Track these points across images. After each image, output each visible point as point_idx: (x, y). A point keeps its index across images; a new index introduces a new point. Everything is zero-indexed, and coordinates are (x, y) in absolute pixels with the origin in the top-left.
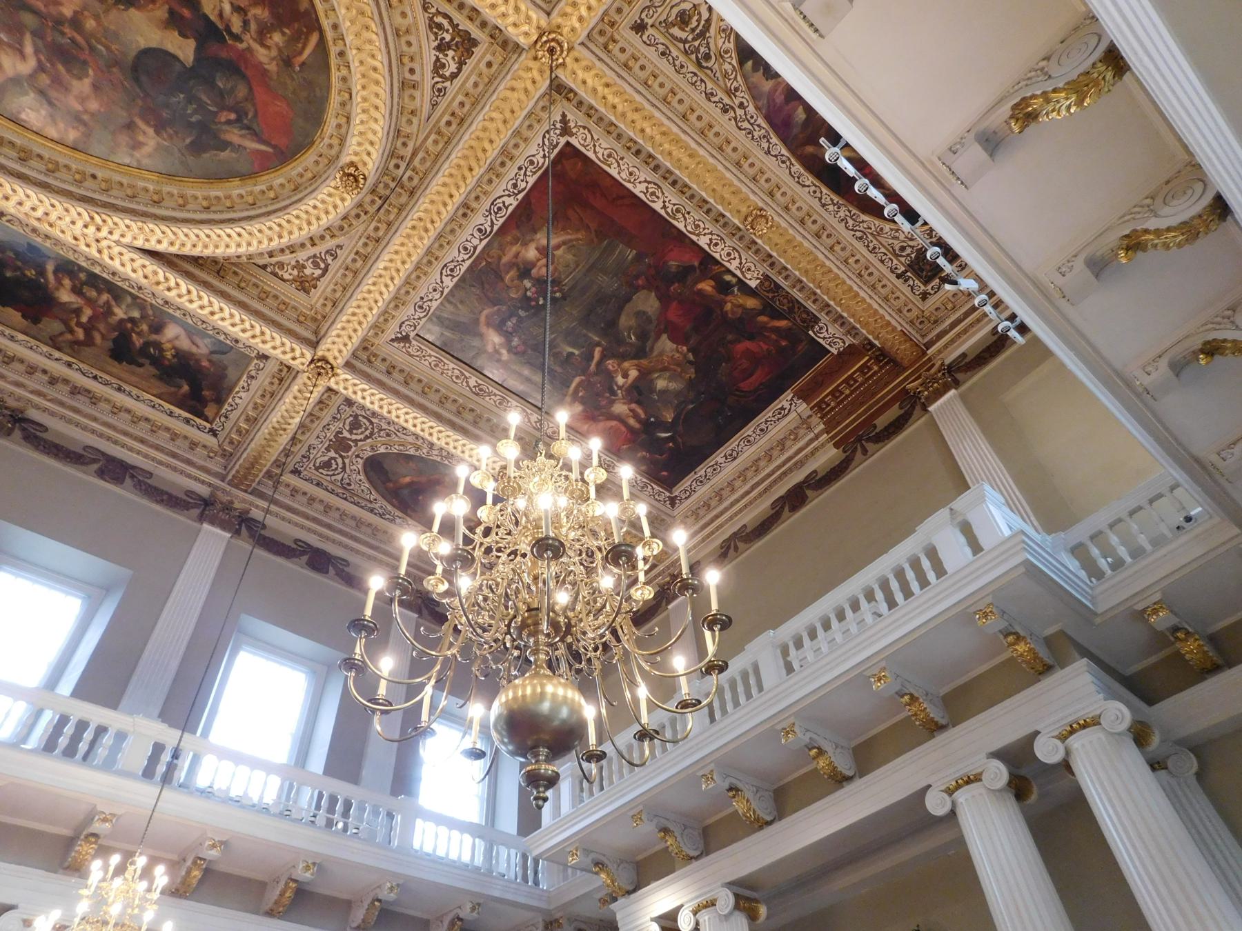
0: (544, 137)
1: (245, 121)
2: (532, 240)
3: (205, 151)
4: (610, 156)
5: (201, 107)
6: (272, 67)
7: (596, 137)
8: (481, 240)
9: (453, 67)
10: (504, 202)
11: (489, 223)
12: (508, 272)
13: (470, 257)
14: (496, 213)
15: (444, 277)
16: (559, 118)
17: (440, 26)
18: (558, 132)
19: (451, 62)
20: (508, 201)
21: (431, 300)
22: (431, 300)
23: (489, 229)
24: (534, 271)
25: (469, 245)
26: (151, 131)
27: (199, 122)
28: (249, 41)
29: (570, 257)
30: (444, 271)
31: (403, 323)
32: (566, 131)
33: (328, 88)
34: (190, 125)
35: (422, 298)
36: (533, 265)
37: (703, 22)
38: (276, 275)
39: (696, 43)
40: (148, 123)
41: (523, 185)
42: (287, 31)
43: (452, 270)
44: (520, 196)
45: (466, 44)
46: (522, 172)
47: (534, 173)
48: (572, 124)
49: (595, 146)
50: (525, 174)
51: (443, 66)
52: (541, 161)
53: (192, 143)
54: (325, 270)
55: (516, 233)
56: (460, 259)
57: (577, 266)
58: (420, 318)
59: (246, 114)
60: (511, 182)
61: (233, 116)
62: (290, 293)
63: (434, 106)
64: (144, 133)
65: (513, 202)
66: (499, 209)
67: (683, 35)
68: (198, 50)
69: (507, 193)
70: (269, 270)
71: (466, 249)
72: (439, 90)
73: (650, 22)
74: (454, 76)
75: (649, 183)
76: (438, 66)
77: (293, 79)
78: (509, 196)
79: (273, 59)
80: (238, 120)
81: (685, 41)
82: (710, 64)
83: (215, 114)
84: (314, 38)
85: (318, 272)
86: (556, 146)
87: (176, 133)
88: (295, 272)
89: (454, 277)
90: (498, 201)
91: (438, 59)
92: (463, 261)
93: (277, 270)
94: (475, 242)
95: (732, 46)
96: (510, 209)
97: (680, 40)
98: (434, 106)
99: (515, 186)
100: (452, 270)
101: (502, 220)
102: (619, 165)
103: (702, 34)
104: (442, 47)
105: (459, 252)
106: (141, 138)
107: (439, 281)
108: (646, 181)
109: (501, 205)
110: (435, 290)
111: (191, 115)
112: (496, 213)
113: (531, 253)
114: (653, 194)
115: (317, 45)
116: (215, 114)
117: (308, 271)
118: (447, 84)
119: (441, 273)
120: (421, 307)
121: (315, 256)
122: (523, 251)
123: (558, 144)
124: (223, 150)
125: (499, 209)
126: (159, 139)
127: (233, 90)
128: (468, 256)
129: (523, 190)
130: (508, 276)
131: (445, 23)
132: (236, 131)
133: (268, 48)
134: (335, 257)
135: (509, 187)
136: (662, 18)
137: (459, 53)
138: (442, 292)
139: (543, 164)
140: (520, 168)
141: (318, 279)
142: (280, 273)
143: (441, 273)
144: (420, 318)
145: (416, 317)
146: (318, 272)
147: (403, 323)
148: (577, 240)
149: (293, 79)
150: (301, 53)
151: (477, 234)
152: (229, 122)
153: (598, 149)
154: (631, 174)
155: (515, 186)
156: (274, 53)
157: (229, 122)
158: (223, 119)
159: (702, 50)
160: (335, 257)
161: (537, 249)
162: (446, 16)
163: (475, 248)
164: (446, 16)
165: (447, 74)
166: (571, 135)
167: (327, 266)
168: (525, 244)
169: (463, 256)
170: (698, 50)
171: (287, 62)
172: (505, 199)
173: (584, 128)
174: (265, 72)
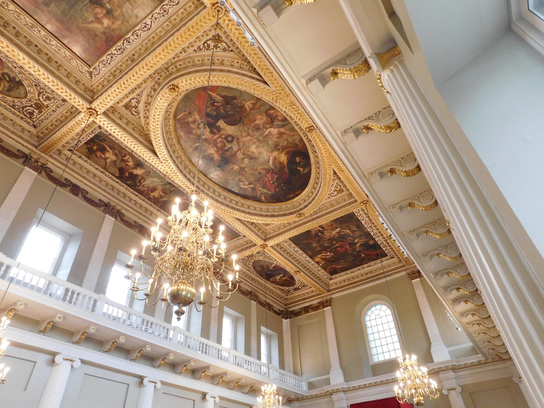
0: (99, 73)
1: (212, 101)
2: (106, 28)
3: (231, 97)
4: (70, 60)
5: (224, 110)
6: (195, 113)
7: (77, 68)
8: (129, 38)
9: (133, 101)
10: (117, 52)
11: (125, 45)
12: (119, 15)
13: (136, 31)
14: (121, 48)
15: (150, 24)
16: (93, 78)
17: (136, 112)
18: (93, 73)
19: (133, 102)
20: (115, 52)
21: (159, 14)
22: (159, 14)
23: (125, 42)
24: (105, 12)
25: (136, 37)
26: (246, 106)
27: (228, 105)
28: (200, 121)
29: (86, 15)
30: (149, 27)
31: (176, 4)
32: (91, 73)
33: (178, 104)
34: (231, 105)
35: (163, 16)
36: (105, 15)
37: (41, 96)
38: (228, 46)
39: (41, 91)
40: (246, 108)
41: (108, 57)
42: (186, 120)
43: (145, 27)
44: (109, 52)
45: (127, 106)
46: (108, 62)
47: (103, 60)
48: (88, 75)
49: (77, 65)
50: (107, 61)
51: (136, 102)
52: (100, 64)
53: (235, 100)
54: (206, 42)
55: (114, 34)
56: (140, 31)
57: (81, 9)
58: (167, 5)
59: (211, 103)
60: (114, 59)
61: (216, 104)
62: (224, 38)
63: (142, 92)
64: (249, 107)
65: (113, 50)
66: (119, 50)
67: (47, 94)
68: (217, 122)
69: (116, 55)
70: (230, 49)
71: (137, 35)
72: (139, 96)
73: (61, 101)
74: (133, 99)
75: (50, 44)
76: (138, 102)
77: (190, 109)
78: (115, 54)
79: (195, 115)
80: (214, 102)
81: (46, 92)
82: (33, 83)
83: (221, 106)
84: (178, 117)
85: (208, 42)
86: (94, 68)
87: (238, 104)
88: (219, 45)
89: (145, 23)
90: (120, 53)
91: (138, 104)
92: (139, 30)
93: (227, 48)
94: (132, 38)
95: (27, 88)
96: (114, 48)
97: (48, 93)
98: (142, 92)
99: (112, 57)
100: (145, 27)
101: (119, 44)
102: (65, 55)
103: (39, 93)
104: (136, 107)
105: (140, 35)
106: (251, 105)
107: (153, 23)
108: (52, 45)
109: (119, 51)
110: (156, 18)
111: (230, 107)
112: (121, 48)
113: (106, 22)
114: (47, 39)
115: (178, 115)
116: (221, 106)
117: (213, 44)
118: (136, 97)
119: (151, 26)
120: (165, 11)
121: (208, 49)
122: (110, 24)
123: (93, 69)
124: (225, 95)
125: (119, 50)
126: (245, 103)
127: (212, 111)
128: (137, 32)
129: (108, 55)
130: (118, 13)
131: (134, 113)
132: (217, 99)
133: (194, 118)
134: (199, 47)
135: (114, 58)
136: (56, 101)
137: (130, 104)
138: (152, 16)
139: (99, 63)
140: (109, 64)
141: (210, 39)
142: (226, 46)
143: (151, 26)
144: (167, 5)
145: (169, 6)
146: (208, 42)
147: (176, 4)
148: (83, 23)
149: (190, 109)
150: (185, 115)
151: (131, 41)
152: (218, 103)
153: (76, 63)
154: (59, 50)
155: (112, 57)
156: (193, 117)
157: (218, 103)
158: (220, 104)
159: (39, 88)
160: (199, 47)
161: (103, 23)
162: (133, 114)
163: (132, 35)
164: (133, 114)
165: (135, 100)
166: (87, 71)
167: (204, 44)
168: (109, 27)
169: (140, 32)
170: (41, 89)
171: (190, 113)
172: (117, 53)
173: (82, 72)
174: (199, 112)
